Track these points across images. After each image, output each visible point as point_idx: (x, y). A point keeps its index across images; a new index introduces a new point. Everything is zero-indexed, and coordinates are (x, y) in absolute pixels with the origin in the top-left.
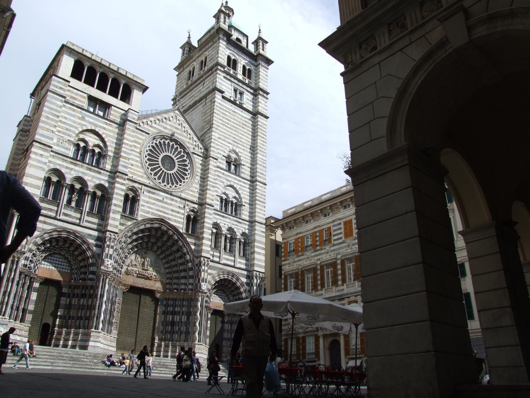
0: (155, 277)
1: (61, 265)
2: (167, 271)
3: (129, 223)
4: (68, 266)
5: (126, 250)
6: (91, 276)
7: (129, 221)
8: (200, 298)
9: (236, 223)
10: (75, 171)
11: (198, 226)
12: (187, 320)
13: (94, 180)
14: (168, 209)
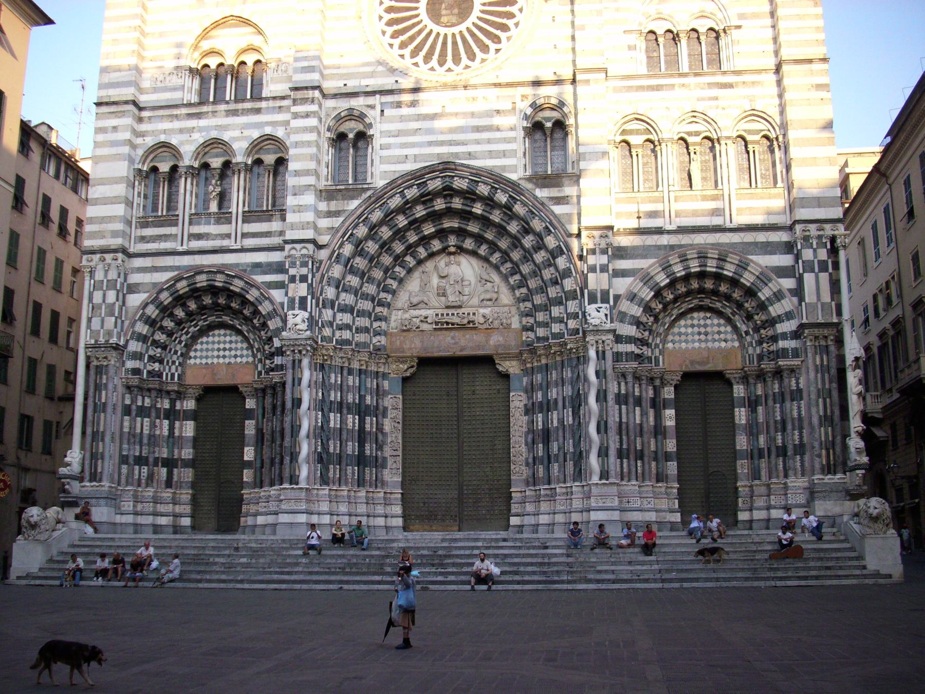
0: (482, 320)
1: (230, 349)
2: (517, 293)
3: (354, 204)
4: (247, 349)
5: (378, 274)
6: (278, 360)
7: (352, 198)
8: (592, 353)
9: (716, 92)
10: (201, 129)
12: (574, 419)
13: (247, 133)
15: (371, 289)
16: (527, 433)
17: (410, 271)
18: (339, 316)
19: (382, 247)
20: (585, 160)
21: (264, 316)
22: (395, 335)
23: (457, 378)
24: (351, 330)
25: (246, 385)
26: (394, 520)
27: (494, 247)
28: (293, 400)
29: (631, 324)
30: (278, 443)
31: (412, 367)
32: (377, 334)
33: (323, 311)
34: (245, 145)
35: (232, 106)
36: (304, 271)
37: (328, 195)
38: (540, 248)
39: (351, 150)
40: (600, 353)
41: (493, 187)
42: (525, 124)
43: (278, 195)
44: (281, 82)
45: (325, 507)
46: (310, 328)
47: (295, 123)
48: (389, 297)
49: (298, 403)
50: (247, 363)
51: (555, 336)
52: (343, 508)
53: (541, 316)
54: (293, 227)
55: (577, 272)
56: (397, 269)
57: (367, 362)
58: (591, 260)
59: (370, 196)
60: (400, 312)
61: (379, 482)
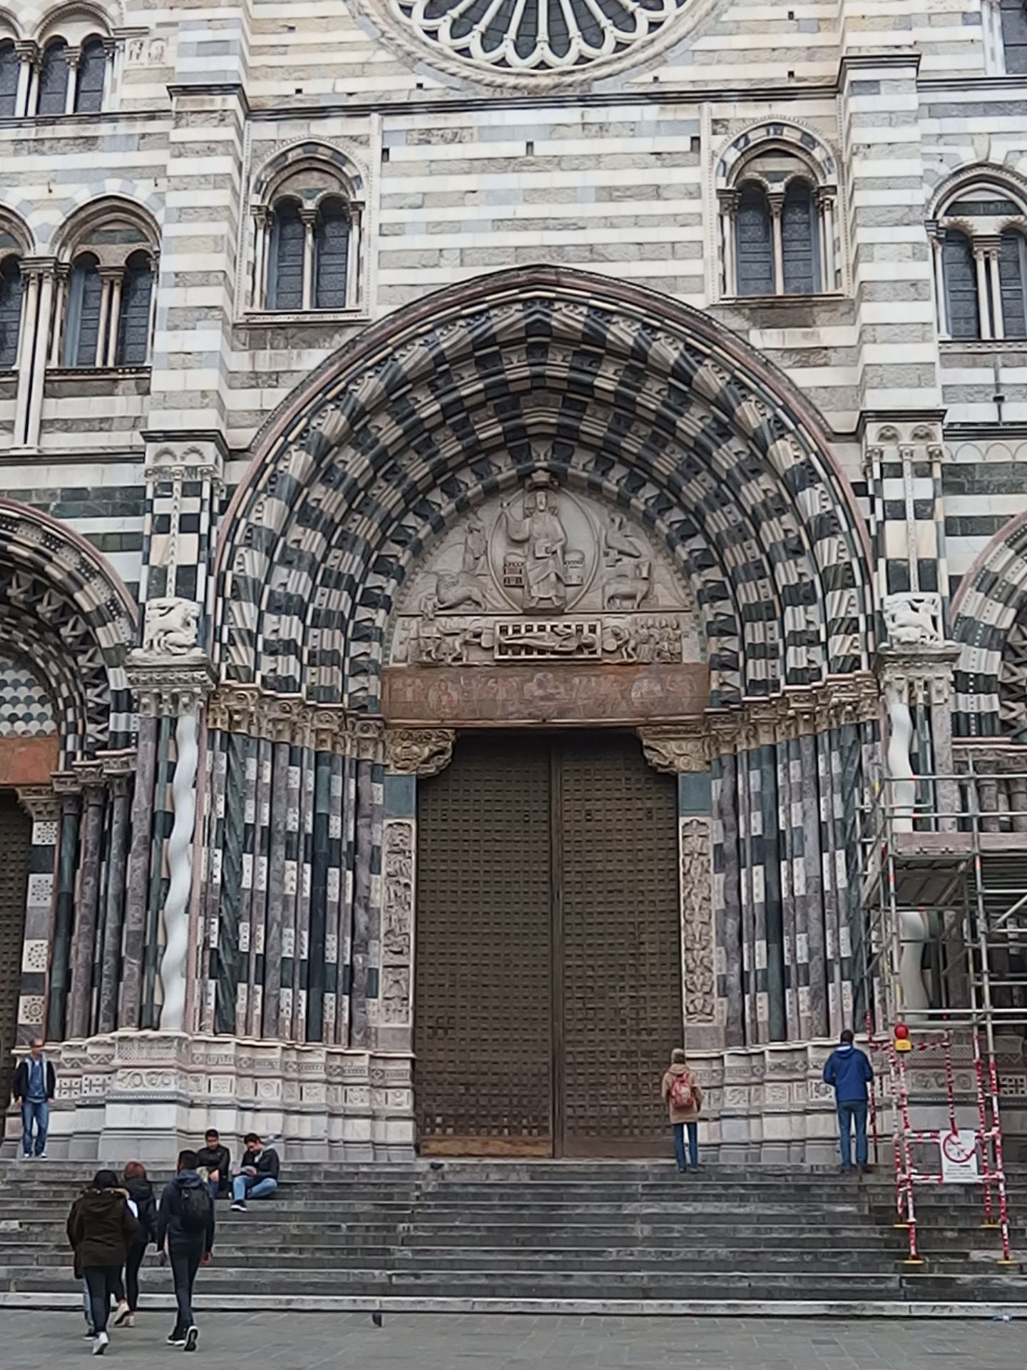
0: (611, 644)
3: (313, 358)
4: (42, 701)
5: (365, 528)
6: (118, 722)
8: (899, 711)
11: (831, 228)
13: (60, 191)
14: (570, 194)
15: (350, 563)
16: (725, 913)
17: (440, 527)
18: (270, 619)
19: (377, 463)
20: (871, 260)
21: (86, 616)
22: (400, 671)
23: (549, 781)
24: (300, 659)
25: (35, 787)
26: (393, 1125)
27: (640, 472)
28: (154, 816)
29: (990, 648)
30: (110, 925)
31: (442, 752)
32: (358, 670)
33: (234, 606)
34: (57, 218)
35: (29, 133)
36: (192, 505)
37: (253, 333)
38: (757, 472)
39: (310, 237)
40: (920, 709)
41: (646, 326)
42: (722, 184)
43: (130, 338)
44: (147, 80)
45: (223, 1089)
46: (201, 640)
47: (178, 167)
48: (390, 586)
49: (163, 823)
50: (40, 733)
51: (796, 676)
52: (270, 1094)
53: (756, 633)
54: (168, 401)
55: (852, 523)
56: (410, 520)
57: (336, 734)
58: (893, 489)
59: (353, 341)
60: (414, 623)
61: (356, 1032)
